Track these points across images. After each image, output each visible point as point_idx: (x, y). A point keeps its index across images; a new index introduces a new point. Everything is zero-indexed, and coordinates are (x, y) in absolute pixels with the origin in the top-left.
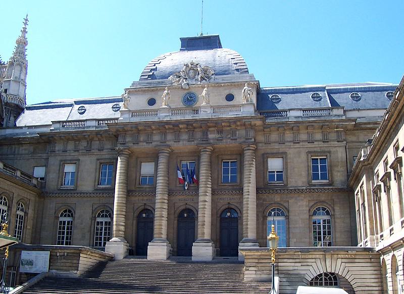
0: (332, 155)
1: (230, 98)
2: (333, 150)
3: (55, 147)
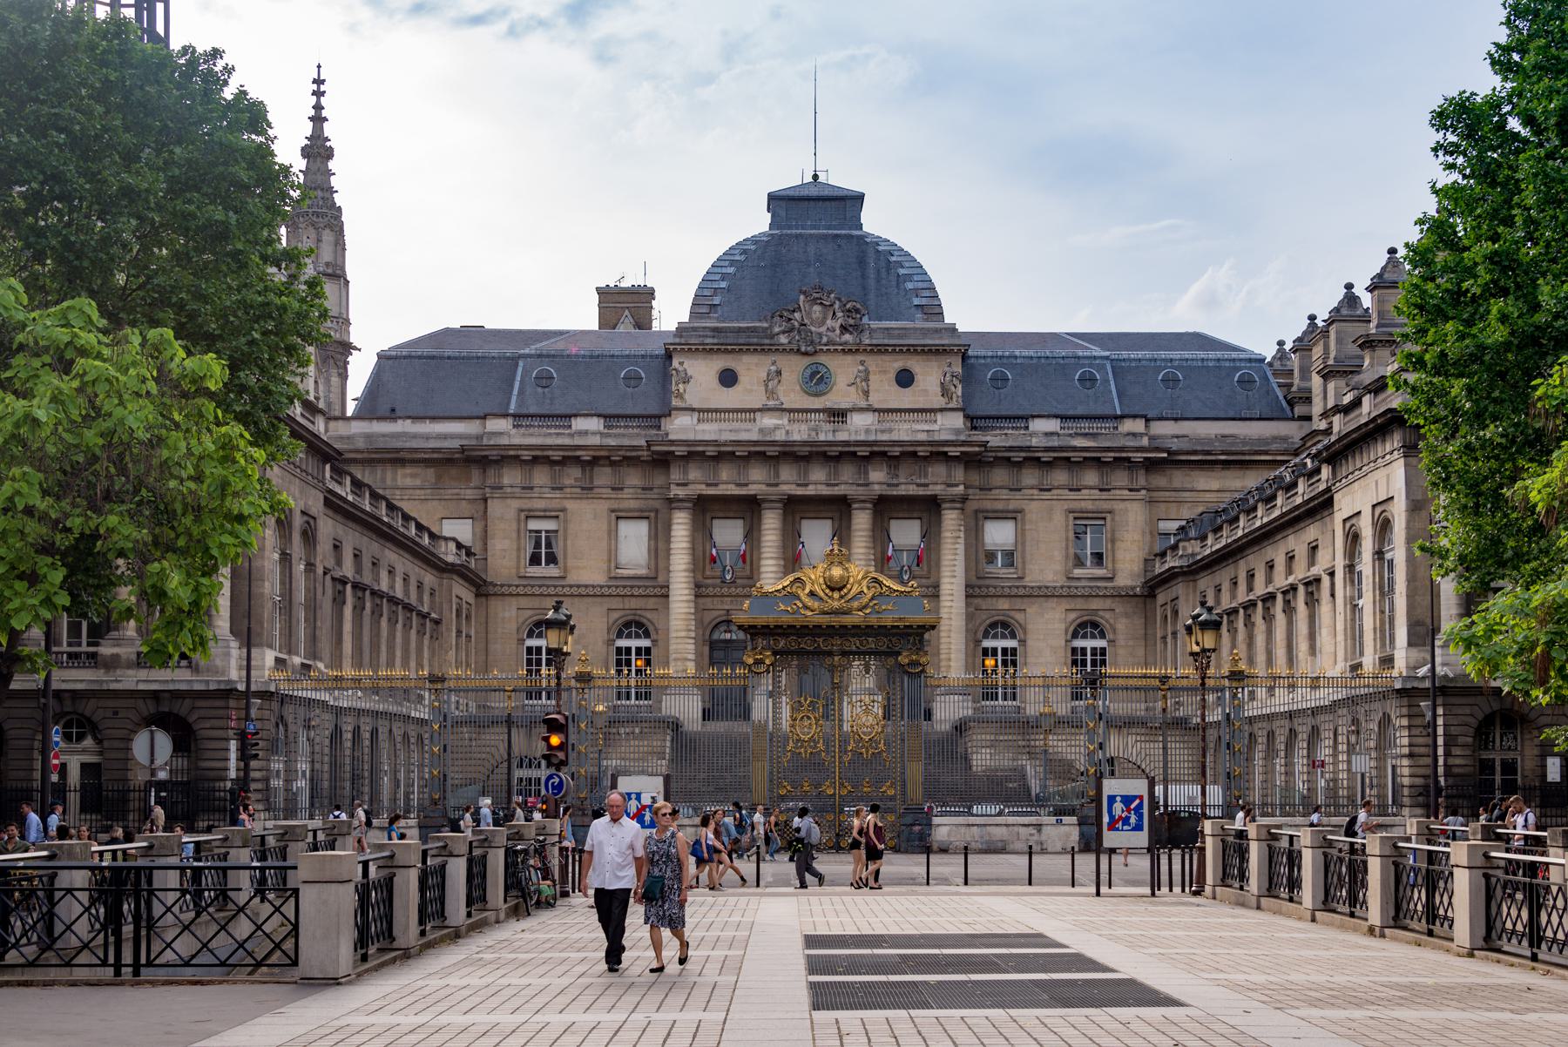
1: (905, 379)
3: (500, 476)
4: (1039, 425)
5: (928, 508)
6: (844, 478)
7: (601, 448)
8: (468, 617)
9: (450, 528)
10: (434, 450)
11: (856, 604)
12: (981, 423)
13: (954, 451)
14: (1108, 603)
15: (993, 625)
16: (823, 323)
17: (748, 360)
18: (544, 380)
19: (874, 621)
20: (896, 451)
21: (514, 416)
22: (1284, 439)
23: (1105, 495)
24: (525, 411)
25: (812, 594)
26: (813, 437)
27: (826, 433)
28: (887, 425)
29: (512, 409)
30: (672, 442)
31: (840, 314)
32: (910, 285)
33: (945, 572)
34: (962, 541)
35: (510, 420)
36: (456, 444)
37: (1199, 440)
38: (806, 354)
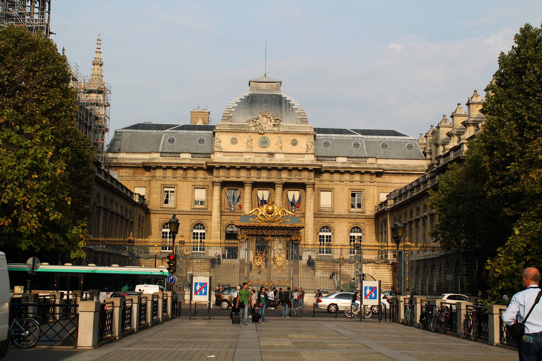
0: (366, 192)
1: (294, 143)
2: (366, 188)
4: (339, 160)
5: (302, 186)
6: (273, 176)
7: (190, 164)
8: (143, 221)
9: (137, 191)
10: (133, 164)
11: (277, 219)
12: (320, 159)
13: (311, 168)
14: (362, 221)
15: (323, 227)
16: (266, 123)
17: (241, 135)
18: (171, 141)
19: (283, 225)
20: (291, 167)
21: (161, 153)
22: (423, 166)
23: (362, 184)
24: (164, 151)
25: (262, 215)
27: (267, 160)
28: (288, 159)
29: (160, 150)
30: (214, 163)
31: (273, 121)
32: (297, 112)
33: (307, 209)
34: (313, 198)
35: (159, 154)
36: (140, 162)
37: (393, 166)
38: (261, 134)
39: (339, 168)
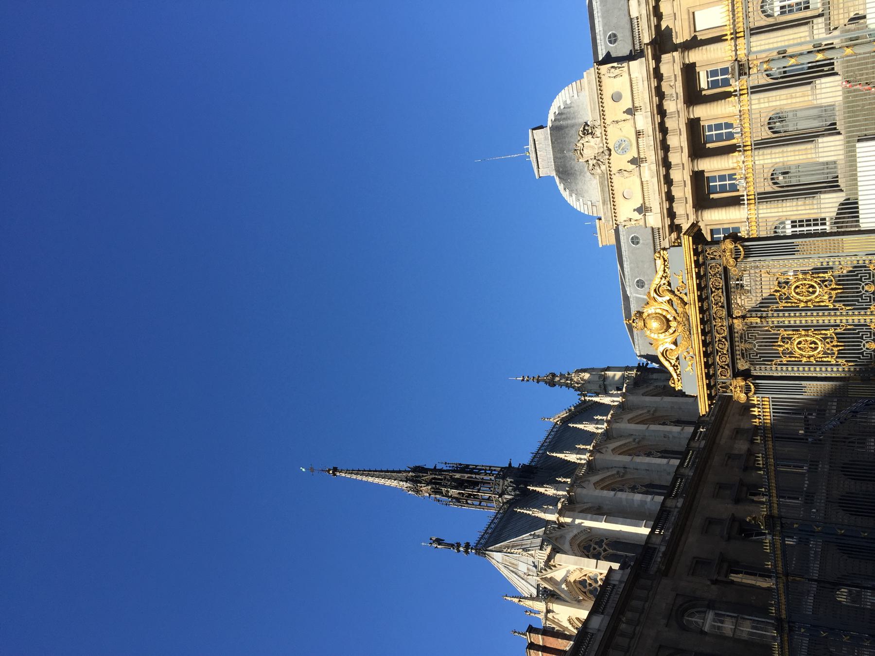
1: (617, 98)
13: (652, 64)
25: (675, 343)
26: (653, 147)
38: (610, 155)
39: (648, 10)
